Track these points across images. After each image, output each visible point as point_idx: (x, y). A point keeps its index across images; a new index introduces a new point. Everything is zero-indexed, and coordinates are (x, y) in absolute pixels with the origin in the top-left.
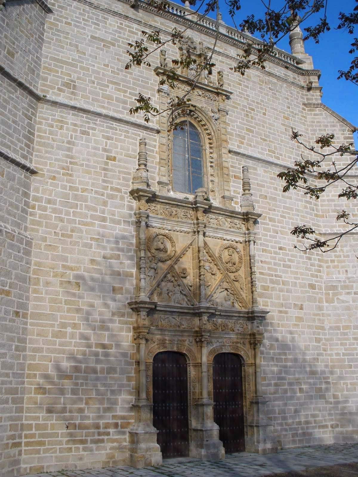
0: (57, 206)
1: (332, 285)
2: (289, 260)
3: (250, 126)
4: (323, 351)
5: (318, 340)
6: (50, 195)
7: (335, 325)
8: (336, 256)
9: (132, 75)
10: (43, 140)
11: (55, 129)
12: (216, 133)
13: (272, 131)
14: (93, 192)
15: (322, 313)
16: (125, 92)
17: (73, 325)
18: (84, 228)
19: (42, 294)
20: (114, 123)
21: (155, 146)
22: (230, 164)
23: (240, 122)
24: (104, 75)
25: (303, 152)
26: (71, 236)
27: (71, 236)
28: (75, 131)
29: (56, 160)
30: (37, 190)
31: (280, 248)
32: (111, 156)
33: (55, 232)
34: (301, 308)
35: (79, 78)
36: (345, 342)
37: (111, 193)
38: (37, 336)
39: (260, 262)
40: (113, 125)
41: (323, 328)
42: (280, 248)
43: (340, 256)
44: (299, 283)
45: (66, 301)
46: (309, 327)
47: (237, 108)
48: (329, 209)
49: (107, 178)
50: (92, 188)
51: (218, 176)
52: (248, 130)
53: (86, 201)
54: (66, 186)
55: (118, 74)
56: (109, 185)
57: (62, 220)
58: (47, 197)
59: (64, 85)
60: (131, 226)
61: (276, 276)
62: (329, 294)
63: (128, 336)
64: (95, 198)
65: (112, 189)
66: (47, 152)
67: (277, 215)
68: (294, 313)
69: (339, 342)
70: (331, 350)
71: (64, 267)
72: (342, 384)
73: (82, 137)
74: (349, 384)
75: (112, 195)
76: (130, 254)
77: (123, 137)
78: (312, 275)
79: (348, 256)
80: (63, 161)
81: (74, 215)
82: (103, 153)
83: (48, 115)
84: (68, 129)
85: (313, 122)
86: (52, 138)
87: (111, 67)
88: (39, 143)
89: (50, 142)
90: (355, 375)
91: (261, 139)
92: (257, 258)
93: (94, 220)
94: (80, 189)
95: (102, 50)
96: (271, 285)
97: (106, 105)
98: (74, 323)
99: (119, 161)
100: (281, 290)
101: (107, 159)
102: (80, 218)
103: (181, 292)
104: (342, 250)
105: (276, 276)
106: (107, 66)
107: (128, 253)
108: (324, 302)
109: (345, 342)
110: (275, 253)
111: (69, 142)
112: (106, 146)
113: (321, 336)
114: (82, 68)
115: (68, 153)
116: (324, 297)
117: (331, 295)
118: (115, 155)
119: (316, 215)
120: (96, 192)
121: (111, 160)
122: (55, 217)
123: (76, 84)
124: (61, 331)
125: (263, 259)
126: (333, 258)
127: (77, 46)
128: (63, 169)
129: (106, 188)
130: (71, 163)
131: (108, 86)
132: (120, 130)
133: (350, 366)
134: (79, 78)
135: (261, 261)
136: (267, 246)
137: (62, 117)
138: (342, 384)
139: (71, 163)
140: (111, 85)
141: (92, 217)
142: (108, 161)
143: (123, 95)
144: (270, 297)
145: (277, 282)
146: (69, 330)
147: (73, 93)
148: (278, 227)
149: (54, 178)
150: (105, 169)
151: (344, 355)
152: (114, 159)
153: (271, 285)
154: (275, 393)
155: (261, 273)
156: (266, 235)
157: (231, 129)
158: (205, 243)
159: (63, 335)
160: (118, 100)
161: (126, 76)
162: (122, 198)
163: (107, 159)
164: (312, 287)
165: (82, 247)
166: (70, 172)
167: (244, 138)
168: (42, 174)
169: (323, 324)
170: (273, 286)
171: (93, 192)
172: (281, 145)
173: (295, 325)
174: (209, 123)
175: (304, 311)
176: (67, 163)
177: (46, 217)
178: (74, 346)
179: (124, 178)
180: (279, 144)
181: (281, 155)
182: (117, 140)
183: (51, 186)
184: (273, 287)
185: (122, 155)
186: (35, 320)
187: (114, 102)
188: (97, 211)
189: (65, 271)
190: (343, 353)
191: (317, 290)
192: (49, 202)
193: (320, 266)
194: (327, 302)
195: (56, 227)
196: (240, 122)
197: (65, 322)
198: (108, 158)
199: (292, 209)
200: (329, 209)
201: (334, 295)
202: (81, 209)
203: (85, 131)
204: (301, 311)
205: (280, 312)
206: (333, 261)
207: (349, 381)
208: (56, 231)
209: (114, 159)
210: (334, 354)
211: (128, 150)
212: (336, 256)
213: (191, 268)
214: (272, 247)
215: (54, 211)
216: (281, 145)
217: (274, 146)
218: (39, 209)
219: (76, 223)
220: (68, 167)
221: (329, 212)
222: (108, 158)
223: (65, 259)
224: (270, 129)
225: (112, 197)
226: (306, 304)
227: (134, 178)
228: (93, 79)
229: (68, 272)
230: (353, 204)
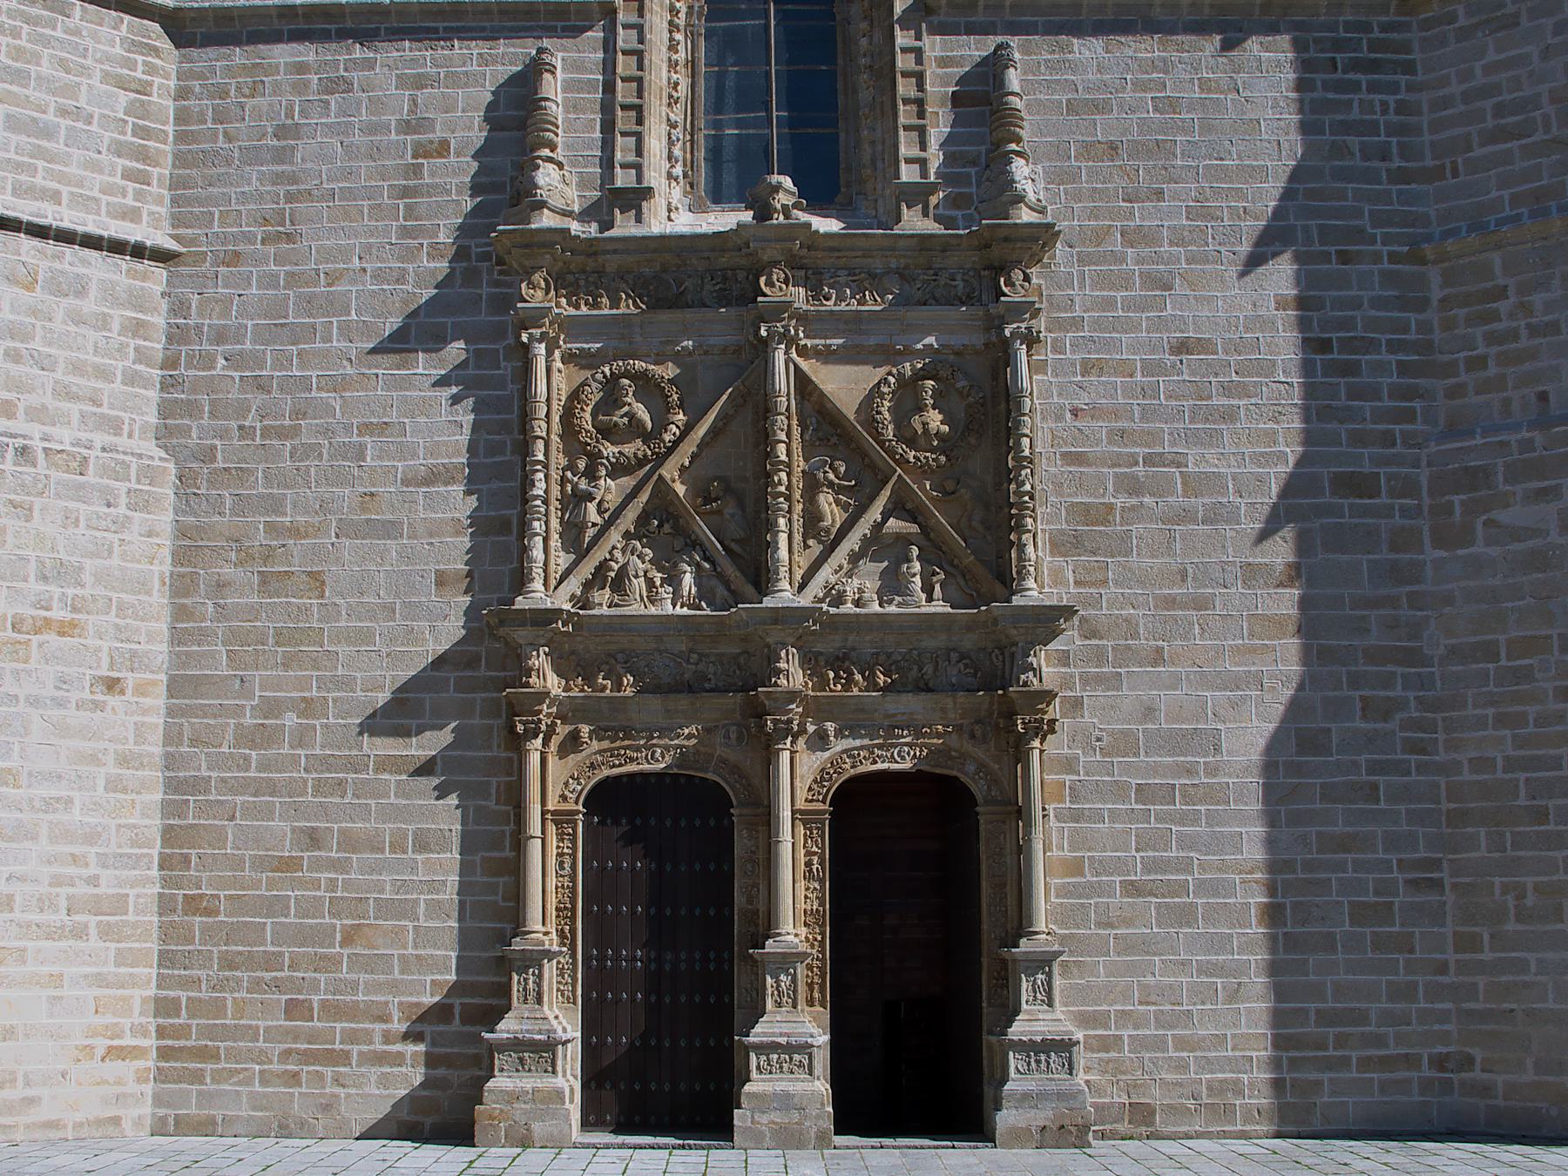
1: (1466, 469)
2: (1227, 390)
4: (1404, 751)
6: (225, 313)
7: (1473, 639)
8: (1491, 339)
27: (295, 431)
28: (300, 88)
29: (244, 198)
31: (1182, 347)
33: (241, 428)
36: (1520, 708)
37: (432, 265)
41: (1412, 657)
42: (1182, 347)
43: (1514, 335)
45: (278, 633)
54: (276, 276)
57: (261, 385)
61: (1149, 460)
62: (1448, 509)
63: (491, 727)
69: (1490, 711)
71: (271, 528)
72: (1497, 892)
74: (1529, 894)
76: (498, 459)
81: (302, 366)
82: (402, 137)
98: (304, 699)
102: (322, 369)
104: (1522, 304)
105: (1149, 460)
107: (493, 456)
109: (1520, 708)
113: (1398, 692)
115: (280, 168)
117: (1458, 510)
119: (1401, 176)
124: (262, 725)
125: (1082, 400)
135: (1075, 412)
138: (1497, 892)
139: (290, 198)
142: (420, 161)
144: (1122, 546)
145: (1161, 489)
146: (291, 720)
149: (235, 258)
151: (1511, 765)
153: (1120, 501)
154: (1128, 922)
166: (288, 228)
173: (1252, 650)
177: (211, 385)
183: (226, 286)
184: (1133, 508)
190: (1507, 758)
191: (1384, 500)
192: (220, 337)
194: (1439, 541)
195: (242, 410)
198: (421, 151)
206: (1479, 363)
207: (1530, 881)
208: (247, 424)
210: (1466, 763)
212: (1492, 339)
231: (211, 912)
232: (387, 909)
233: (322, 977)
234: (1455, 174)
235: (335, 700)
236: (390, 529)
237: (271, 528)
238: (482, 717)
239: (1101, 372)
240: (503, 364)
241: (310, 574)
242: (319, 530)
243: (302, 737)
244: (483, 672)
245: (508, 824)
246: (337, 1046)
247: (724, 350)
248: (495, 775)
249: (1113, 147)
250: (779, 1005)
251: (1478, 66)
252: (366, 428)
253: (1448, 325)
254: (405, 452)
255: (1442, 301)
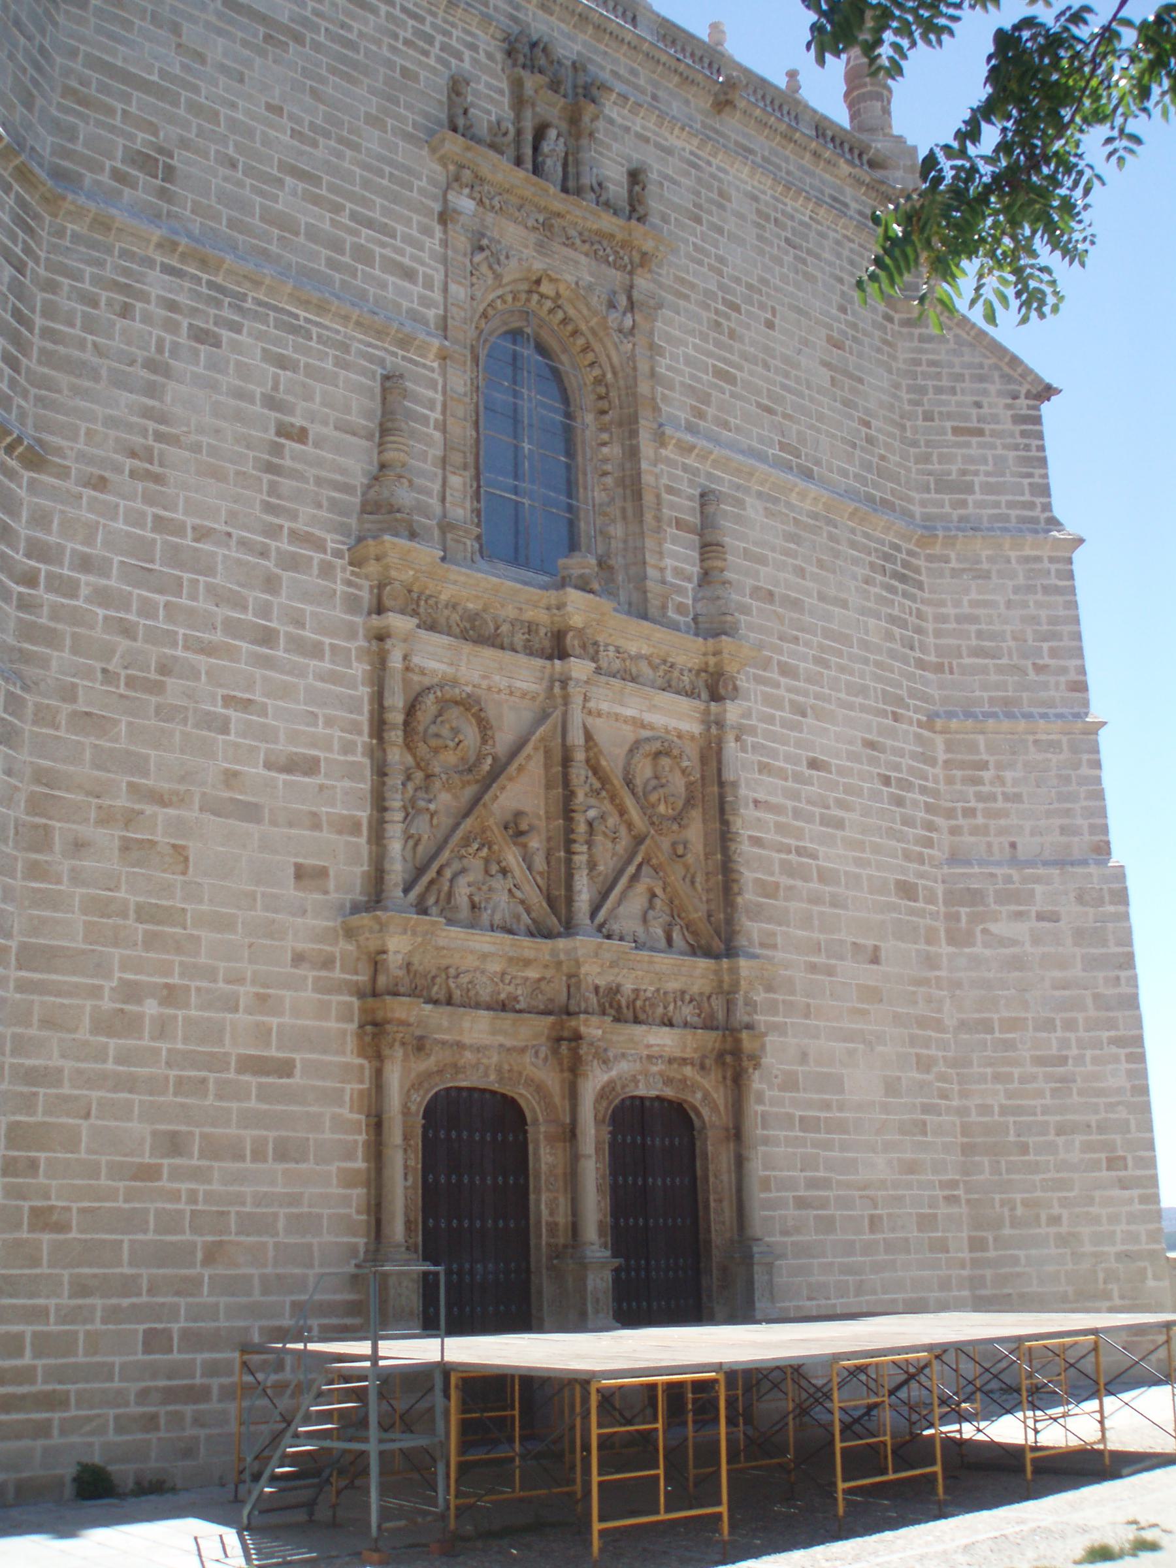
0: (113, 583)
2: (841, 804)
3: (721, 359)
5: (924, 1064)
6: (89, 540)
7: (976, 1016)
8: (980, 797)
9: (360, 152)
10: (61, 349)
11: (103, 313)
12: (620, 375)
13: (792, 384)
14: (233, 543)
15: (938, 978)
16: (337, 209)
17: (165, 992)
18: (202, 662)
19: (59, 882)
20: (302, 314)
21: (431, 406)
22: (665, 481)
23: (695, 346)
24: (266, 141)
25: (883, 458)
26: (157, 688)
27: (157, 688)
28: (171, 326)
29: (111, 422)
30: (41, 519)
31: (814, 764)
32: (292, 425)
33: (105, 671)
34: (875, 960)
35: (184, 144)
36: (1008, 1069)
38: (40, 1028)
39: (751, 805)
40: (296, 317)
41: (938, 1025)
42: (814, 764)
43: (992, 797)
44: (870, 878)
45: (139, 908)
46: (897, 1019)
47: (686, 298)
48: (959, 647)
49: (279, 497)
50: (230, 530)
51: (624, 518)
52: (719, 373)
53: (210, 571)
55: (315, 145)
56: (287, 524)
57: (127, 631)
58: (79, 547)
59: (133, 162)
60: (355, 664)
62: (956, 917)
63: (344, 1033)
64: (239, 562)
65: (294, 535)
66: (76, 391)
67: (804, 658)
68: (855, 972)
69: (989, 1070)
70: (964, 1094)
71: (133, 788)
73: (196, 353)
75: (294, 556)
77: (329, 365)
78: (907, 856)
79: (1017, 798)
80: (130, 427)
81: (169, 618)
83: (81, 261)
84: (147, 318)
85: (917, 362)
86: (95, 345)
87: (291, 117)
88: (47, 358)
89: (88, 356)
90: (1037, 1178)
91: (759, 405)
92: (743, 791)
93: (235, 637)
94: (189, 530)
95: (263, 53)
96: (785, 881)
97: (274, 248)
98: (167, 986)
99: (317, 445)
100: (816, 899)
101: (279, 433)
102: (190, 627)
103: (510, 891)
104: (998, 777)
106: (277, 110)
108: (943, 942)
109: (1008, 1069)
110: (798, 778)
111: (151, 365)
112: (275, 388)
113: (933, 1052)
114: (195, 108)
115: (151, 402)
116: (941, 926)
118: (305, 424)
119: (921, 664)
120: (243, 543)
121: (288, 436)
122: (106, 618)
123: (174, 162)
124: (122, 1010)
125: (760, 796)
126: (972, 804)
127: (176, 29)
128: (133, 454)
129: (273, 532)
130: (159, 437)
131: (280, 182)
132: (319, 336)
133: (1024, 1149)
134: (184, 144)
135: (756, 802)
136: (774, 754)
137: (126, 272)
139: (159, 437)
140: (289, 181)
141: (231, 627)
142: (282, 440)
143: (332, 219)
146: (151, 1008)
147: (163, 194)
148: (806, 694)
149: (101, 484)
150: (270, 468)
151: (1004, 1111)
152: (301, 435)
153: (785, 881)
155: (757, 842)
156: (770, 719)
157: (669, 368)
158: (588, 737)
159: (132, 1025)
160: (313, 234)
161: (340, 156)
162: (327, 570)
163: (279, 433)
164: (907, 890)
165: (197, 725)
166: (156, 469)
167: (706, 399)
168: (60, 465)
169: (939, 1011)
170: (791, 882)
171: (233, 543)
172: (818, 431)
174: (601, 340)
175: (883, 968)
176: (145, 437)
177: (76, 617)
178: (169, 1064)
179: (333, 503)
180: (811, 427)
181: (818, 463)
182: (310, 371)
185: (325, 423)
186: (35, 970)
187: (302, 239)
188: (244, 608)
189: (137, 807)
190: (1001, 1106)
192: (85, 564)
193: (930, 826)
194: (952, 940)
195: (107, 652)
196: (695, 346)
197: (136, 983)
199: (845, 639)
200: (959, 647)
201: (974, 919)
202: (193, 597)
203: (207, 332)
204: (874, 967)
205: (813, 968)
206: (970, 813)
208: (110, 668)
209: (301, 435)
211: (347, 409)
212: (980, 797)
213: (542, 813)
214: (788, 758)
215: (103, 597)
216: (818, 431)
217: (799, 433)
218: (49, 588)
219: (174, 644)
220: (149, 450)
221: (960, 656)
222: (283, 431)
223: (138, 765)
224: (787, 375)
225: (293, 563)
226: (888, 946)
227: (364, 504)
228: (231, 151)
229: (149, 809)
230: (1035, 632)
231: (62, 1227)
232: (250, 1224)
233: (182, 1301)
234: (951, 673)
235: (198, 989)
236: (250, 812)
237: (133, 788)
238: (338, 1020)
239: (770, 774)
240: (355, 664)
241: (174, 846)
242: (181, 800)
243: (162, 1029)
244: (337, 974)
245: (360, 1133)
246: (198, 1381)
247: (524, 695)
248: (349, 1082)
249: (771, 594)
250: (597, 1312)
251: (966, 599)
252: (228, 701)
253: (950, 781)
254: (266, 734)
255: (946, 762)
